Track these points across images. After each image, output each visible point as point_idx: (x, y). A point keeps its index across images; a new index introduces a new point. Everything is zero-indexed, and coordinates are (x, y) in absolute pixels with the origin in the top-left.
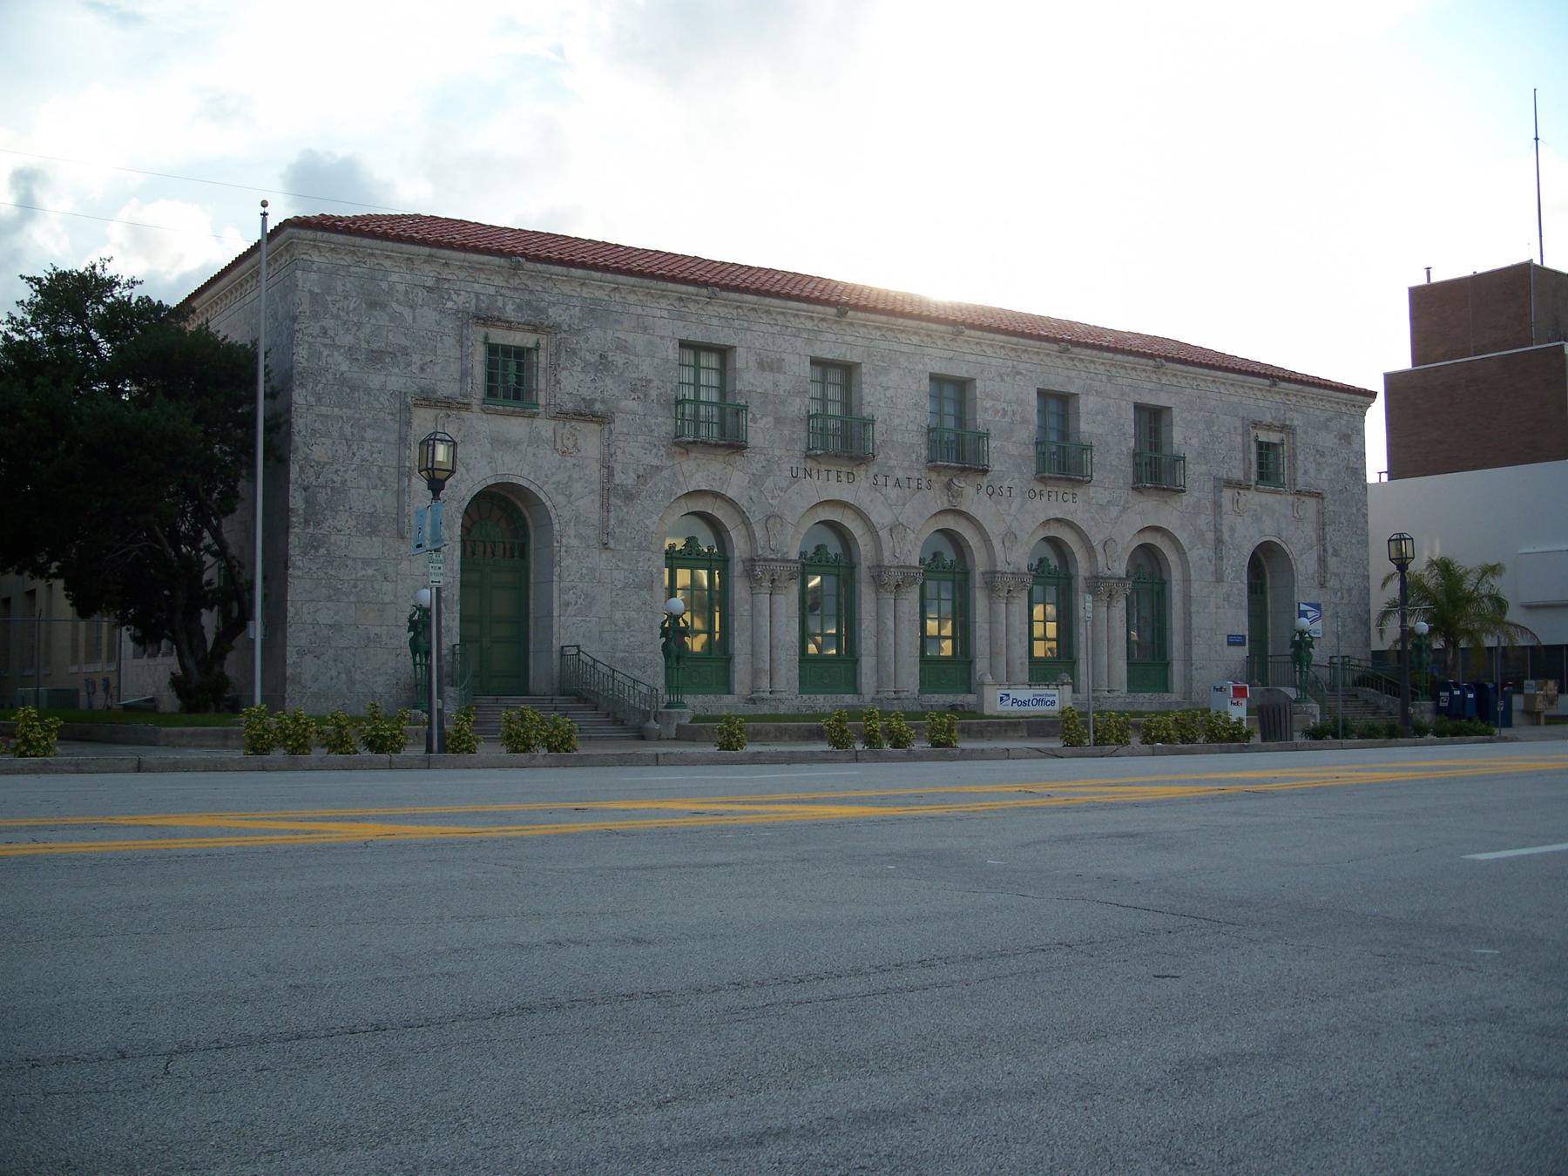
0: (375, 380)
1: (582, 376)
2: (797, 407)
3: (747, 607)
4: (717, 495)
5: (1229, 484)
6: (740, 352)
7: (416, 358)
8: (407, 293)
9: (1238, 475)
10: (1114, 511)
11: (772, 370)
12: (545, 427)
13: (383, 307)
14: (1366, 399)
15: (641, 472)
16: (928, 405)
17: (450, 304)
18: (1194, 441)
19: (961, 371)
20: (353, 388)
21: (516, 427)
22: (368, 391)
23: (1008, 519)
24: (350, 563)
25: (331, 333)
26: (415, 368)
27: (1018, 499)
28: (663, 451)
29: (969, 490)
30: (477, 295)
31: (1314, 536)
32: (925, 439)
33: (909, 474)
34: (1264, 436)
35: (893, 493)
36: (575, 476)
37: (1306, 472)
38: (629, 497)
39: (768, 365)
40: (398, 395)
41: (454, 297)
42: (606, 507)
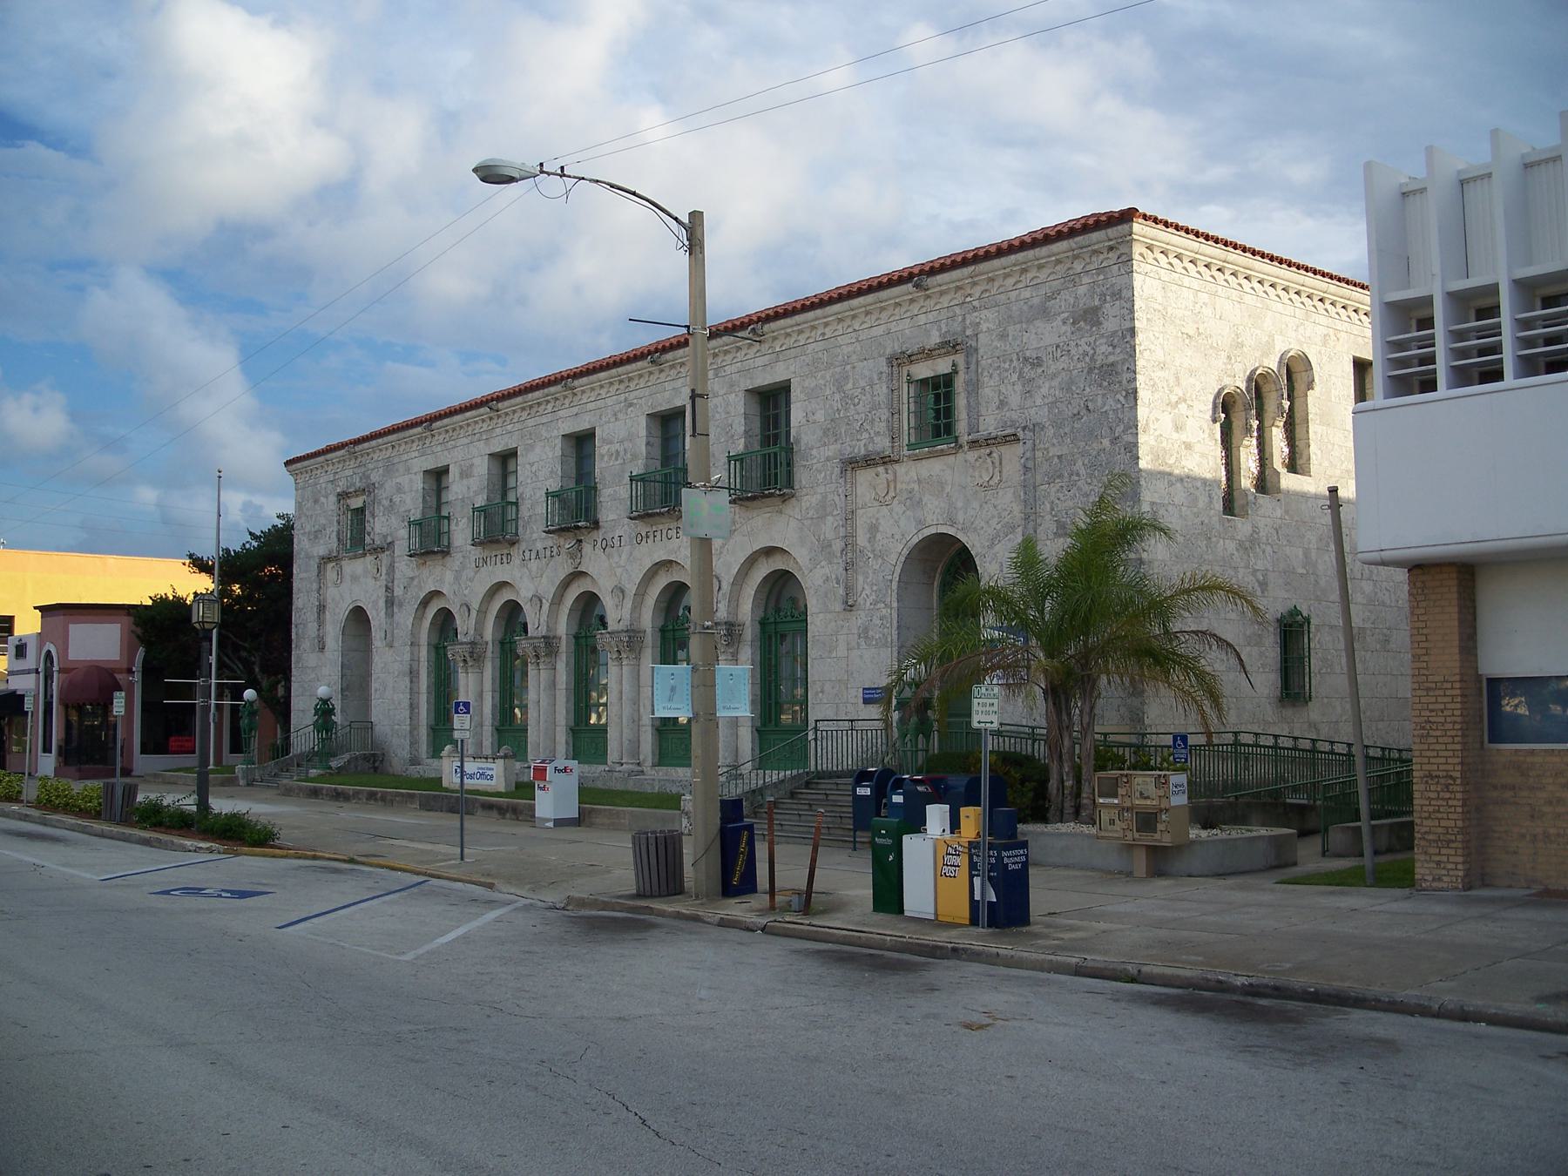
5: (869, 462)
9: (882, 444)
14: (1112, 232)
18: (820, 416)
23: (619, 571)
31: (1017, 509)
34: (923, 370)
35: (534, 565)
37: (1002, 404)
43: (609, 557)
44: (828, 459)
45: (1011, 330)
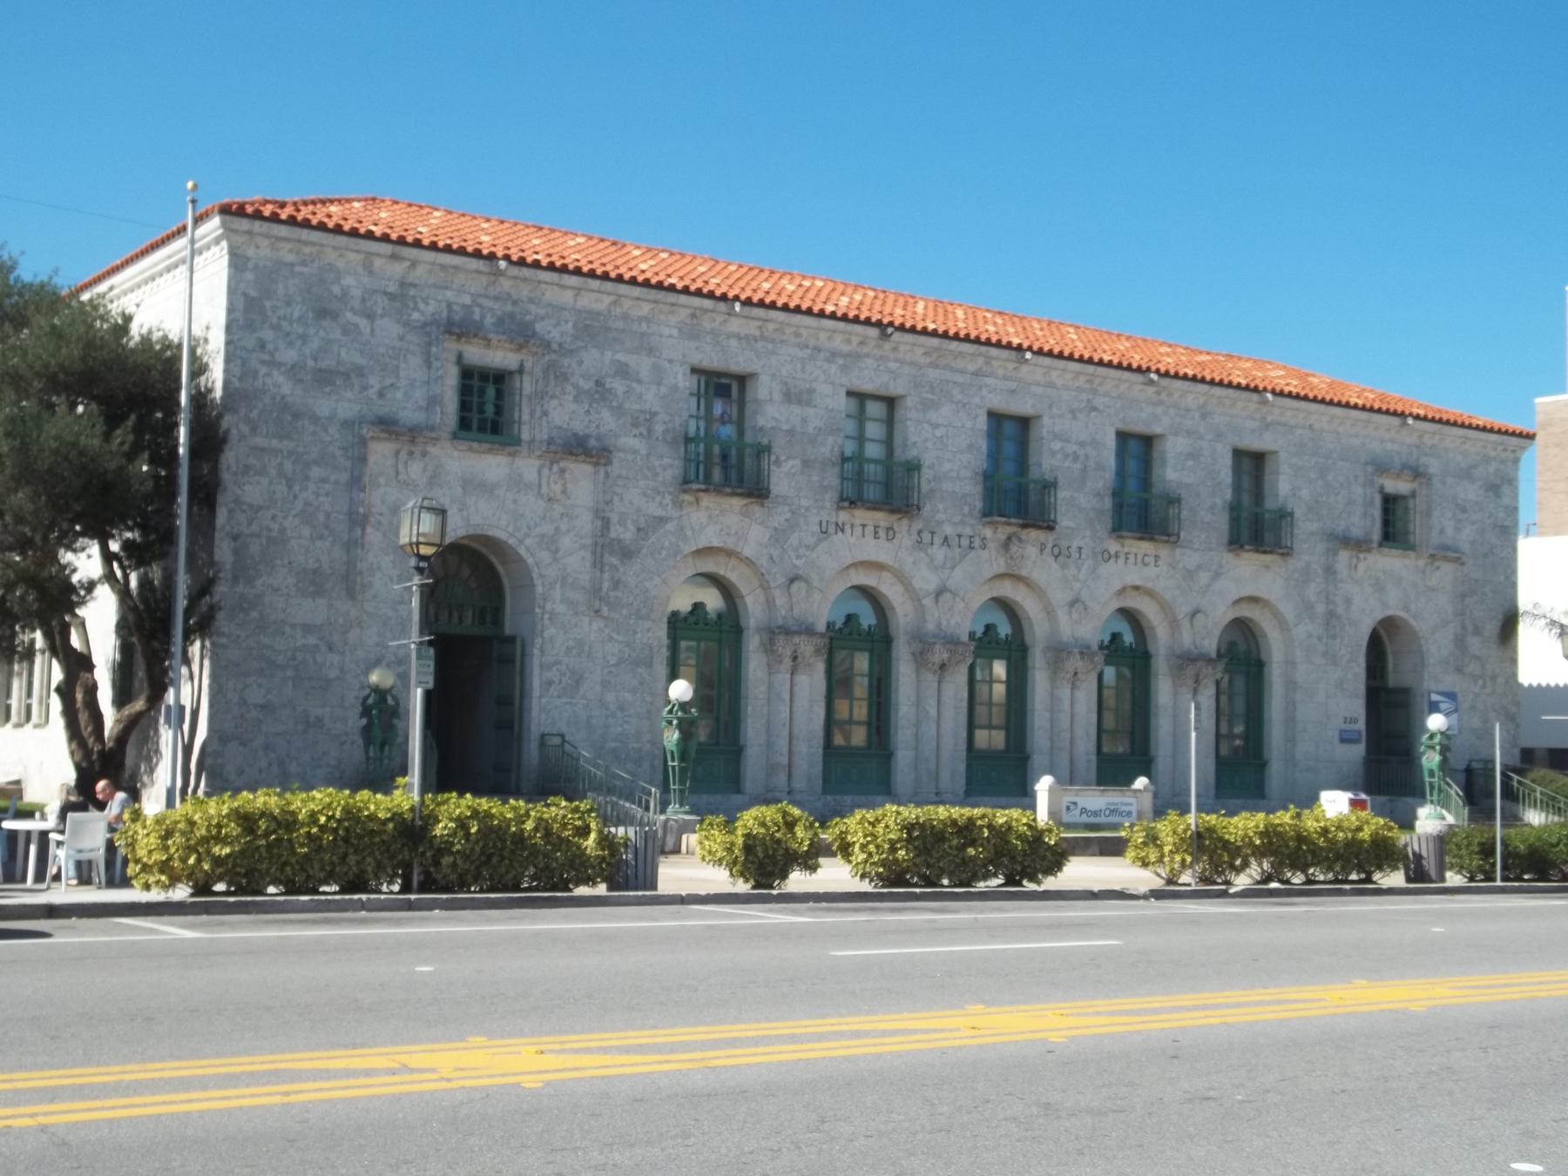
0: (323, 405)
1: (573, 407)
2: (828, 448)
3: (763, 689)
4: (729, 553)
6: (764, 379)
7: (374, 382)
8: (364, 300)
9: (1356, 532)
10: (1204, 578)
11: (800, 402)
12: (528, 467)
13: (334, 315)
15: (642, 524)
16: (983, 445)
17: (416, 316)
18: (1305, 493)
19: (1022, 407)
20: (297, 416)
21: (492, 465)
22: (315, 419)
24: (287, 629)
25: (270, 347)
26: (372, 393)
27: (1089, 563)
28: (668, 499)
29: (1031, 551)
30: (449, 305)
32: (979, 488)
33: (960, 530)
35: (939, 553)
36: (563, 527)
37: (1442, 531)
38: (627, 554)
39: (792, 396)
40: (347, 424)
41: (422, 306)
42: (598, 563)
43: (1064, 566)
44: (1312, 534)
45: (1450, 480)
